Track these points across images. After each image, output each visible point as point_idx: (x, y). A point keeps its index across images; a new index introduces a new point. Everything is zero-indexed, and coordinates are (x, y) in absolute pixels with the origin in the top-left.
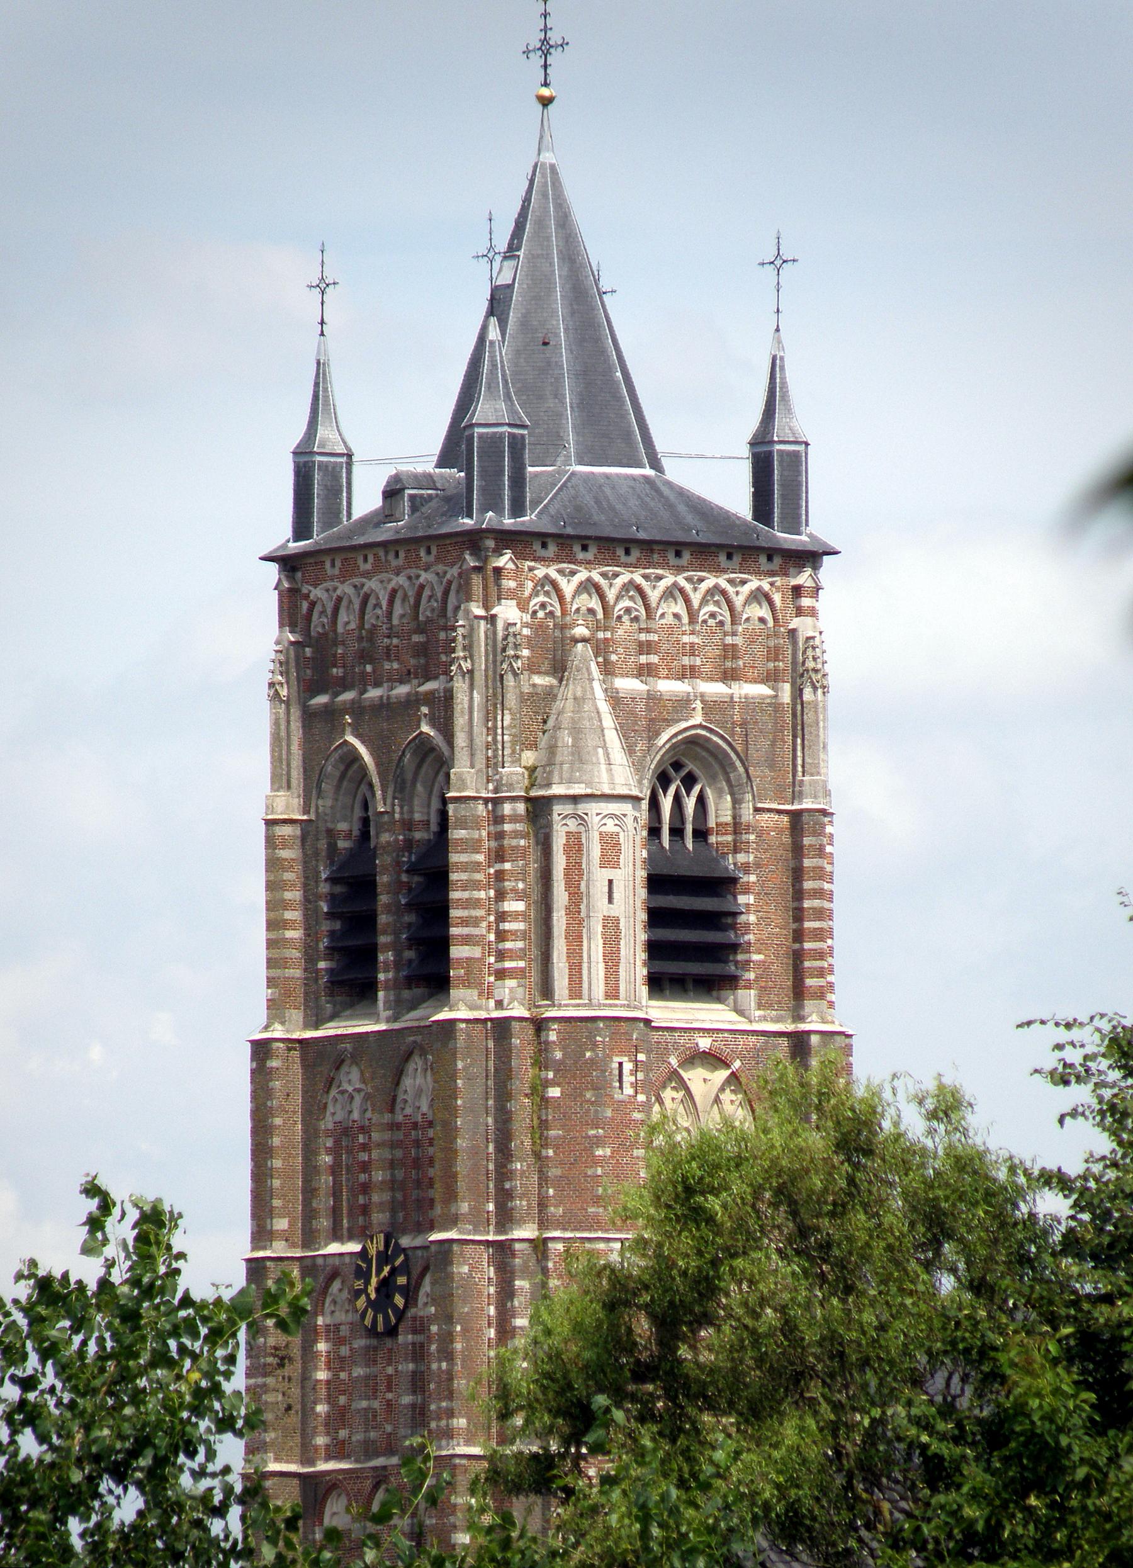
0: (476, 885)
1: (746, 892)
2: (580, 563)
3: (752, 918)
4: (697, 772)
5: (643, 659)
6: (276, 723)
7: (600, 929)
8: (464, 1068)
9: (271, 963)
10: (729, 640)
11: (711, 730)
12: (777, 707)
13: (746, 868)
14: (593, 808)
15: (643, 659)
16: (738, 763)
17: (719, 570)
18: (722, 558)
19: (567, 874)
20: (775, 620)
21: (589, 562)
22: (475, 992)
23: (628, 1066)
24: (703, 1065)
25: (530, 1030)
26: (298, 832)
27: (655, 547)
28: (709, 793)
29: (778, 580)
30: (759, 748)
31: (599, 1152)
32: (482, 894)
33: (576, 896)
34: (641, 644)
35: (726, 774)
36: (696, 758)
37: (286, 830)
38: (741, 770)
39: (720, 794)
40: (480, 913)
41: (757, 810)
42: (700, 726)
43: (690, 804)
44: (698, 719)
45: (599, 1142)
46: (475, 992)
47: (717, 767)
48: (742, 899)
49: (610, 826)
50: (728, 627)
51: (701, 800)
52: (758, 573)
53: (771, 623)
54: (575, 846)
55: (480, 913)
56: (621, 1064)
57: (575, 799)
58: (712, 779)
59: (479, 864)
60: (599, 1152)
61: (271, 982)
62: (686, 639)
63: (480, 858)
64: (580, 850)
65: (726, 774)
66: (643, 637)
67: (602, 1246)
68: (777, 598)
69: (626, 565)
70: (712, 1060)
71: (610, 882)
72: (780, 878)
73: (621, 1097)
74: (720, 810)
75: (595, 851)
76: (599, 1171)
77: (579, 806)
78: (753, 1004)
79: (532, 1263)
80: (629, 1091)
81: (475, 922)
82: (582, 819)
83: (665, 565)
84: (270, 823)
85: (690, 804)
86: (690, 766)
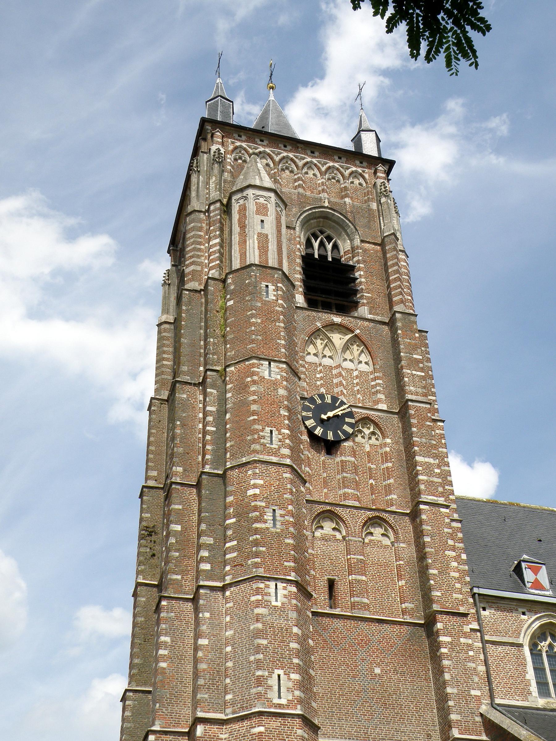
0: (200, 243)
1: (359, 269)
2: (259, 145)
3: (363, 280)
4: (332, 234)
5: (296, 184)
6: (165, 293)
7: (256, 237)
8: (187, 310)
9: (157, 375)
10: (343, 186)
11: (334, 210)
12: (370, 210)
13: (358, 262)
14: (250, 192)
15: (296, 184)
16: (350, 224)
17: (334, 161)
18: (336, 158)
19: (239, 220)
20: (366, 183)
21: (264, 146)
22: (197, 283)
23: (271, 287)
24: (339, 333)
25: (221, 285)
26: (172, 327)
27: (299, 145)
28: (339, 242)
29: (367, 170)
30: (361, 222)
31: (254, 320)
32: (202, 247)
33: (243, 226)
34: (296, 179)
35: (346, 231)
36: (330, 227)
37: (166, 326)
38: (352, 227)
39: (344, 241)
40: (202, 254)
41: (362, 241)
42: (327, 207)
43: (329, 247)
44: (326, 204)
45: (252, 316)
46: (197, 283)
47: (341, 230)
48: (357, 274)
49: (262, 200)
50: (342, 182)
51: (335, 247)
52: (355, 166)
53: (364, 185)
54: (243, 210)
55: (202, 254)
56: (267, 286)
57: (241, 190)
58: (339, 235)
59: (201, 236)
60: (254, 320)
61: (156, 382)
62: (320, 182)
63: (202, 234)
64: (245, 210)
65: (346, 231)
66: (296, 177)
67: (255, 361)
68: (366, 176)
69: (284, 150)
70: (344, 330)
71: (262, 221)
72: (377, 267)
73: (267, 299)
74: (345, 246)
75: (251, 206)
76: (253, 328)
77: (244, 193)
78: (366, 312)
79: (219, 382)
80: (272, 297)
81: (199, 257)
82: (246, 198)
83: (307, 155)
84: (159, 325)
85: (329, 247)
86: (328, 232)
